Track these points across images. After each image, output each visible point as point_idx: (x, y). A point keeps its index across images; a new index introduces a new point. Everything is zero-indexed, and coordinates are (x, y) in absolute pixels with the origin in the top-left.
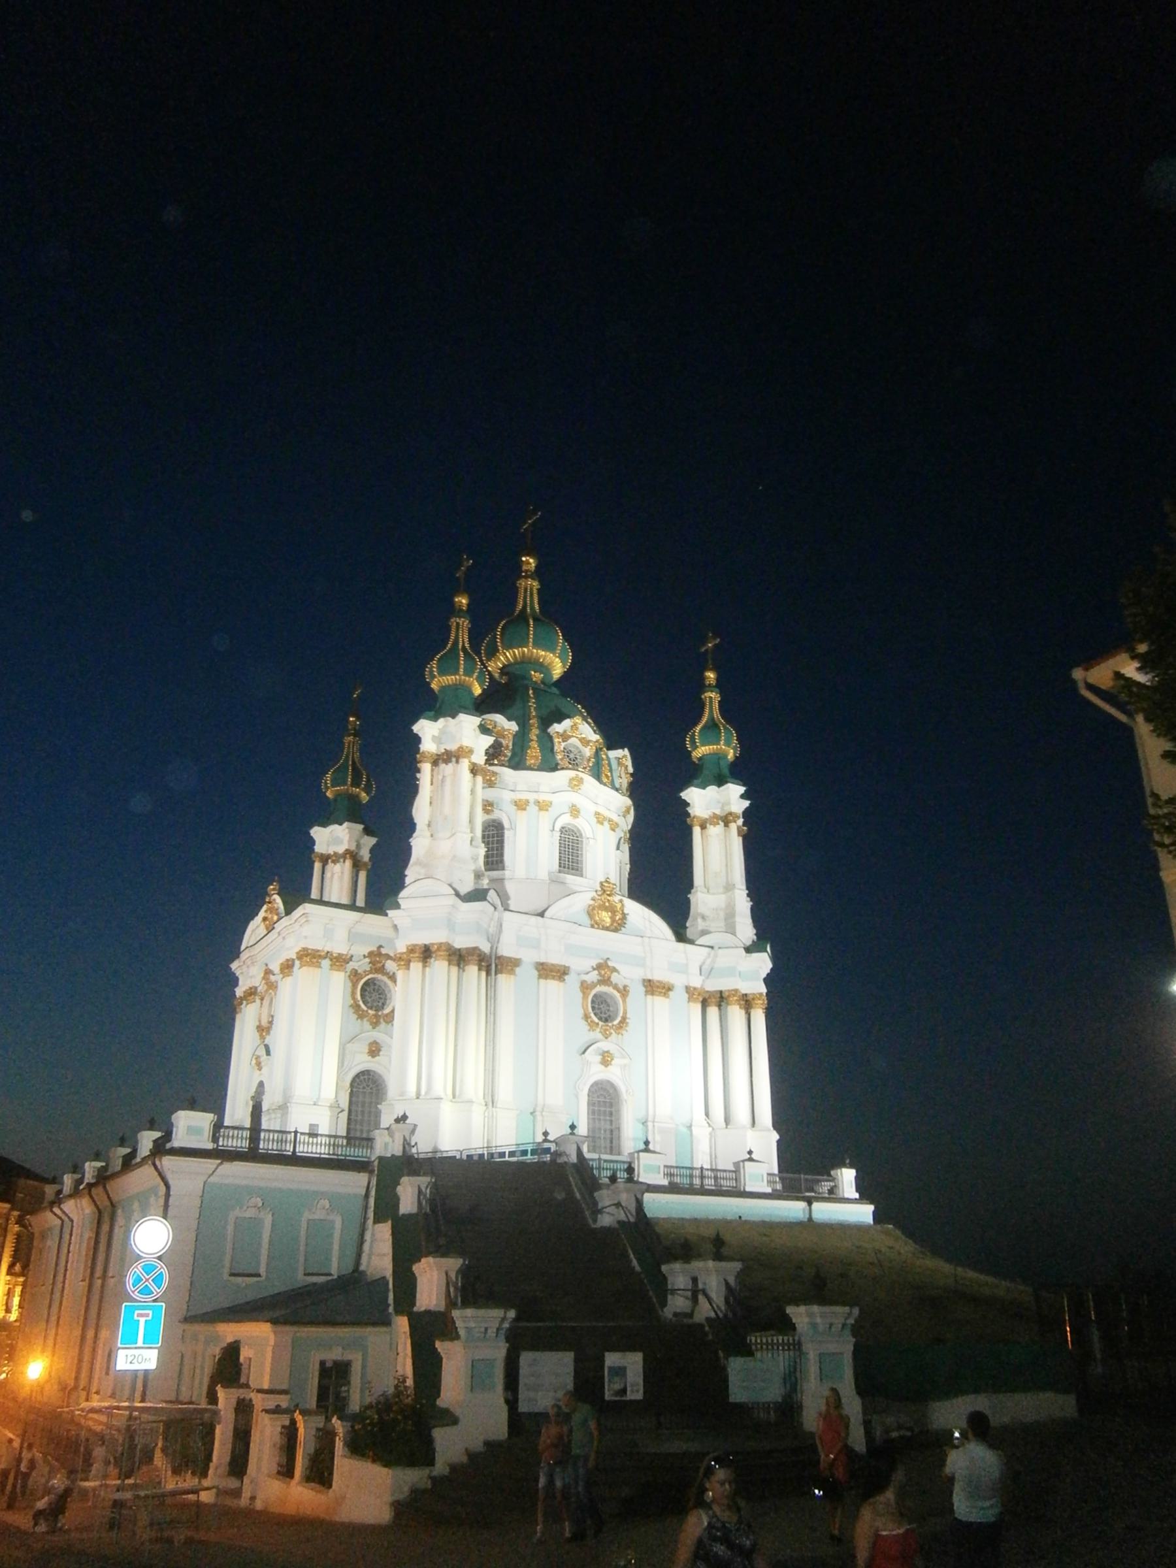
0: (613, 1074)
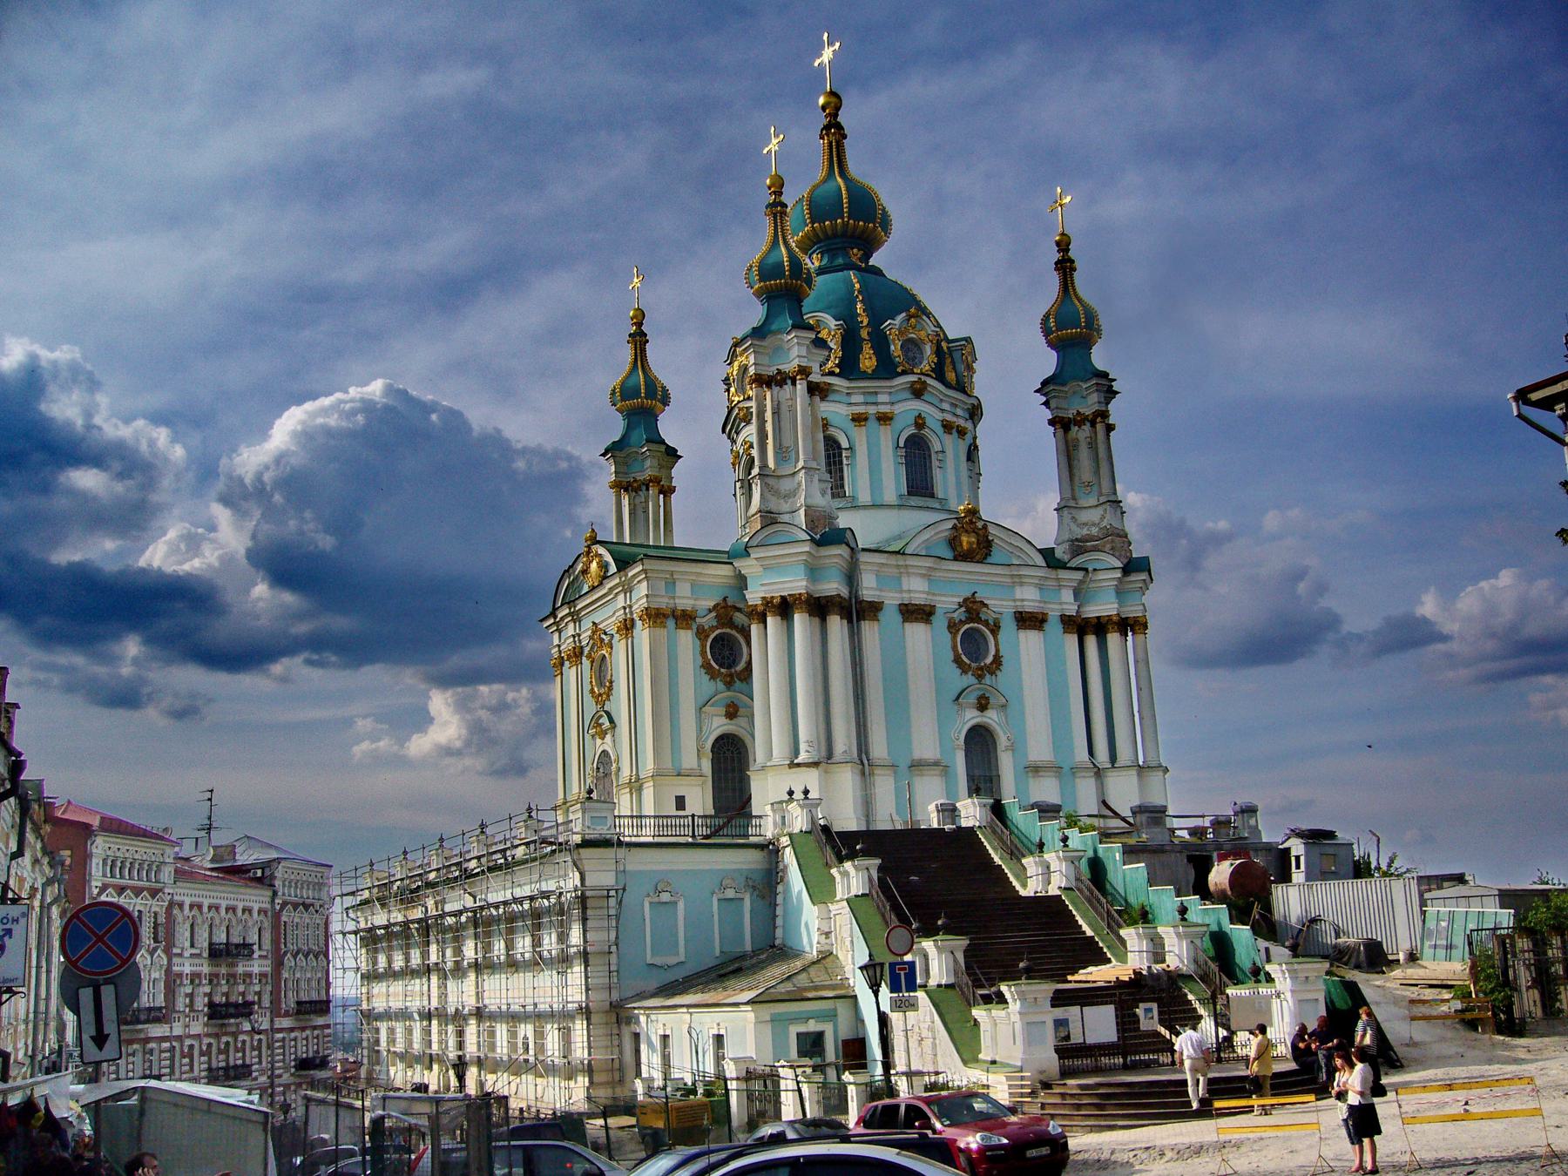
0: (992, 718)
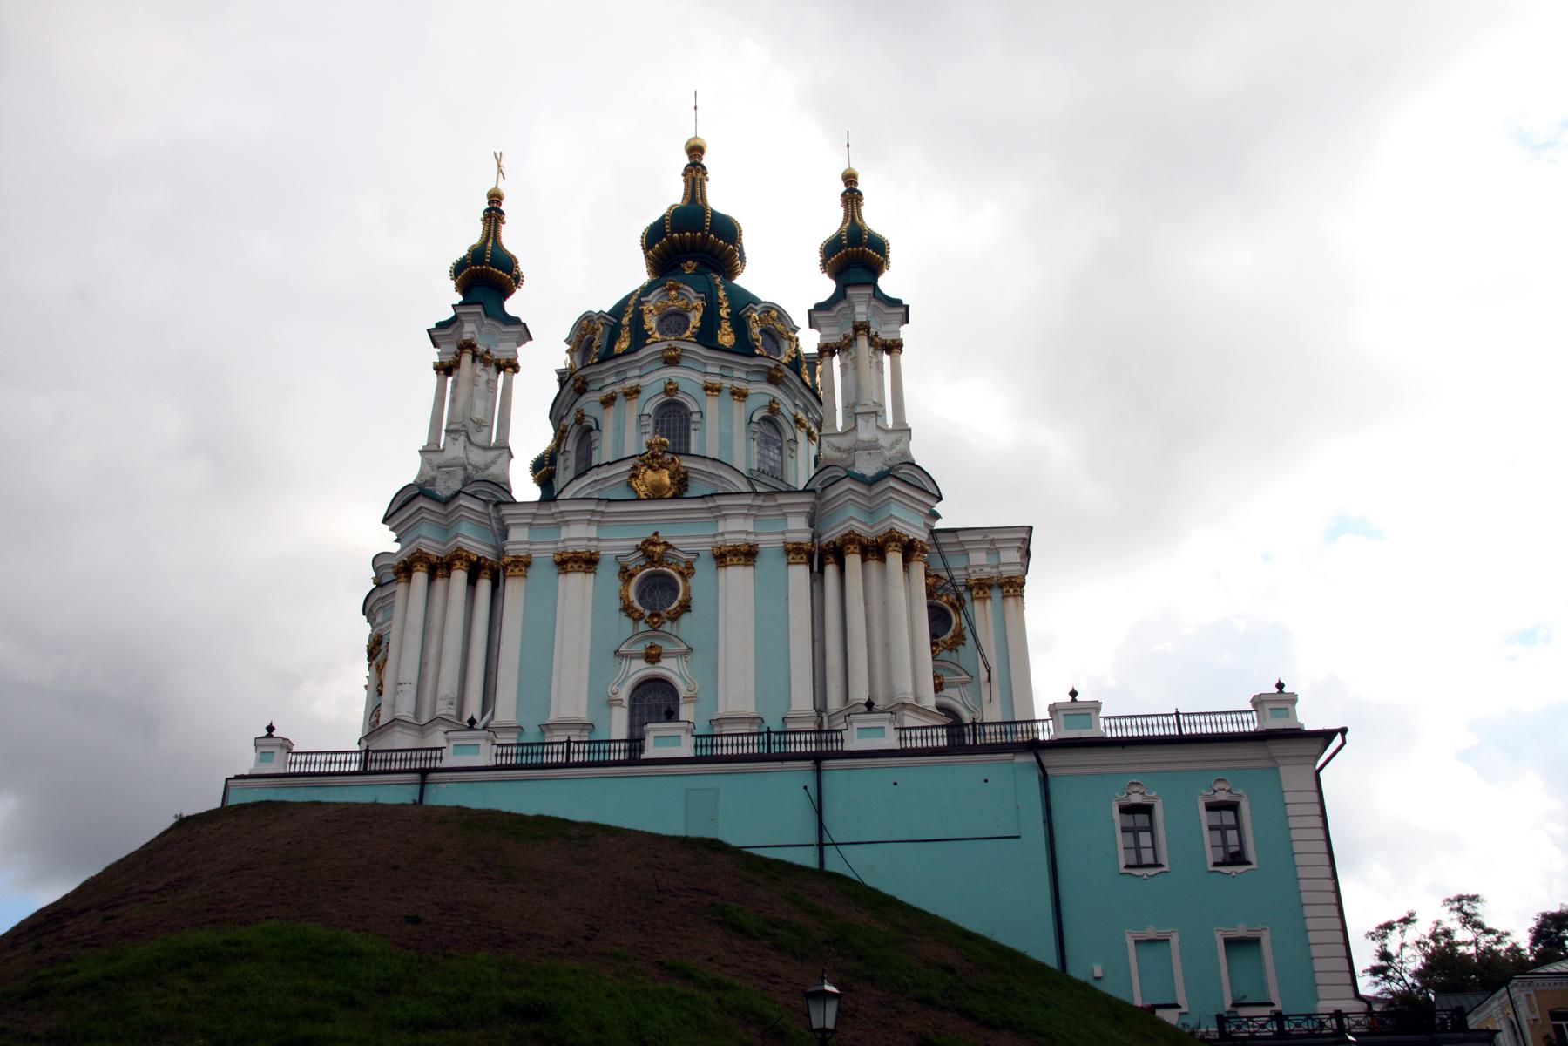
0: (669, 668)
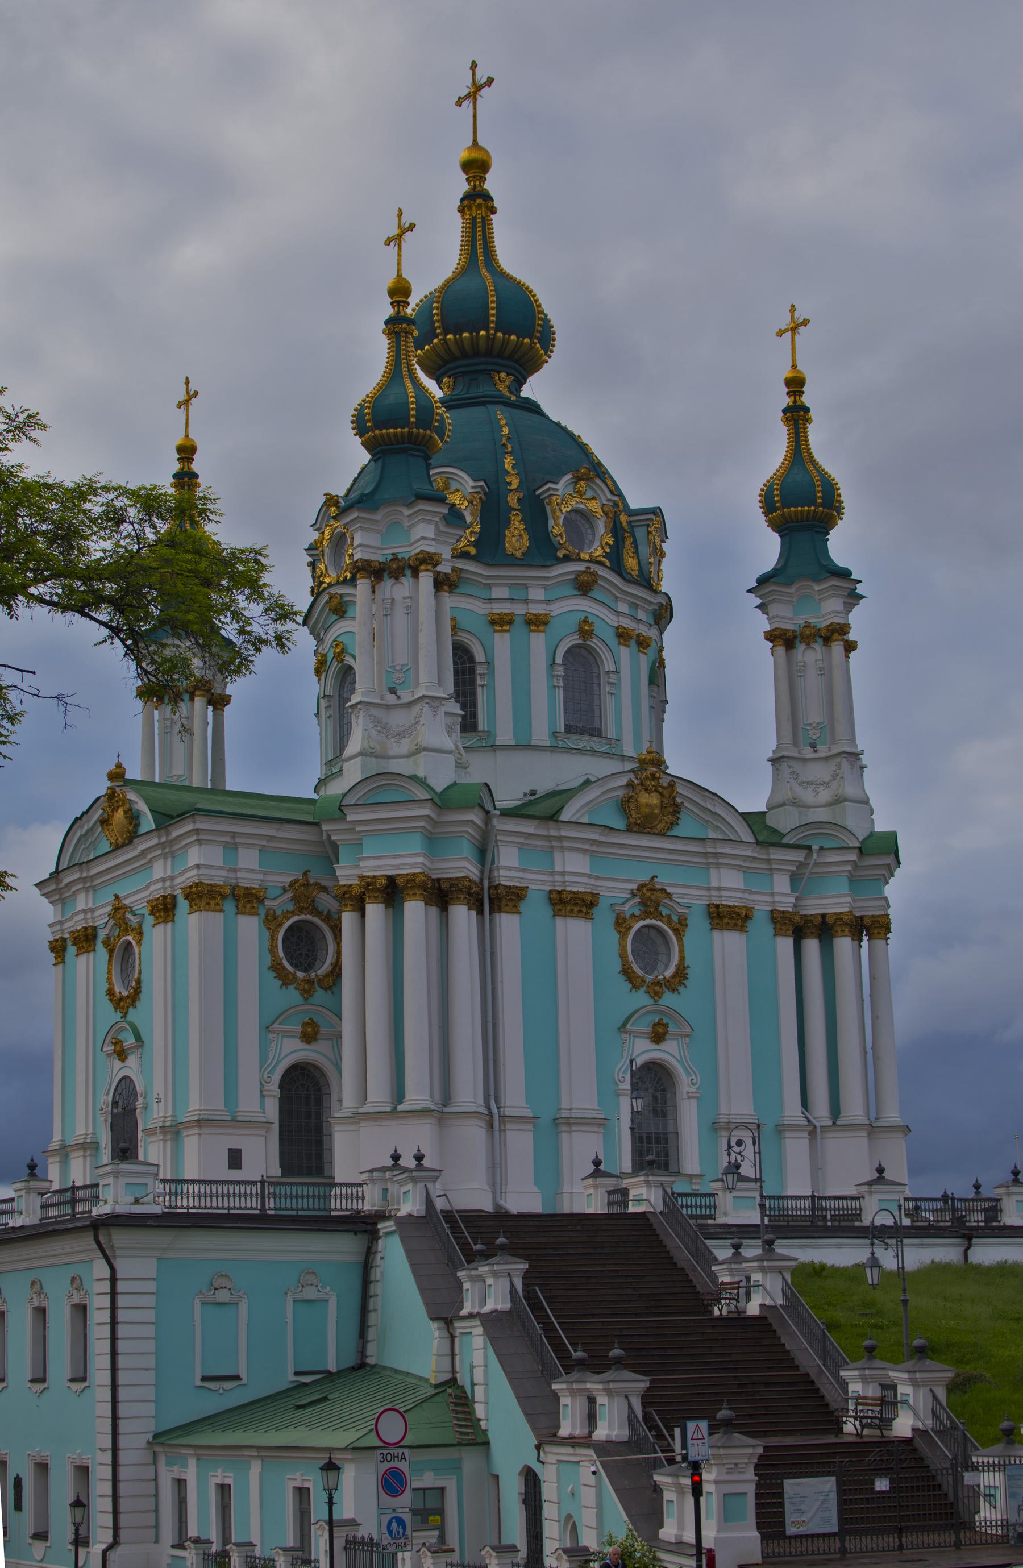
0: (669, 1052)
